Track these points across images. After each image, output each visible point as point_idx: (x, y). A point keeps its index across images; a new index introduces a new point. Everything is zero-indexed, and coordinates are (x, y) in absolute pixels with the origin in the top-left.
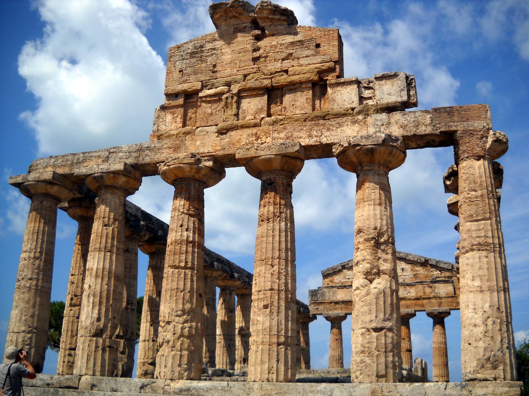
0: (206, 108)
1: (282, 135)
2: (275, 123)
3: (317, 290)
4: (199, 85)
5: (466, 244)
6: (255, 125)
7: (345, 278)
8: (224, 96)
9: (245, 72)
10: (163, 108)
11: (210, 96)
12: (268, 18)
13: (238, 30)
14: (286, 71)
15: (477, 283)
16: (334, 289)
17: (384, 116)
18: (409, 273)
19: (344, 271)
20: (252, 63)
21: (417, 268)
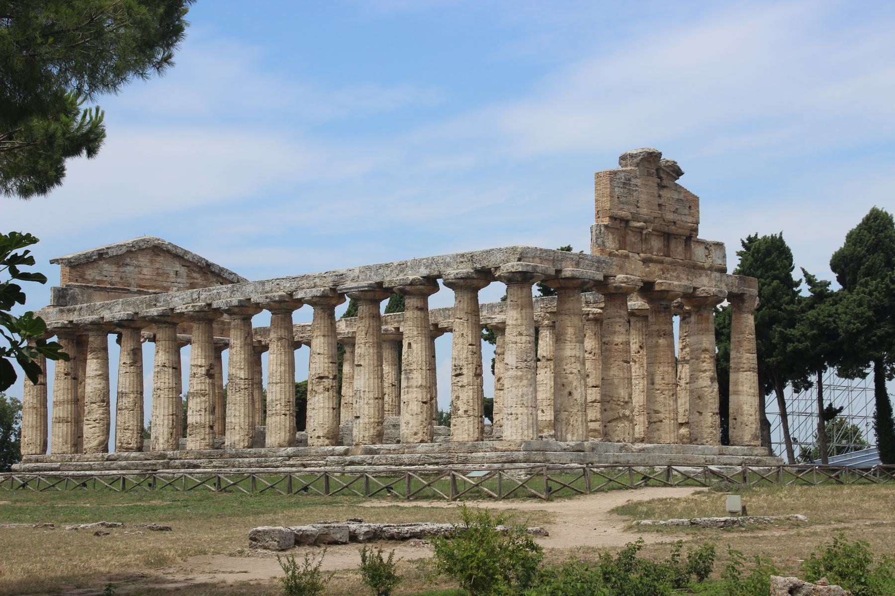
0: (632, 238)
1: (675, 274)
2: (671, 263)
3: (66, 289)
4: (630, 217)
5: (745, 366)
6: (662, 262)
7: (100, 274)
8: (644, 232)
9: (655, 215)
10: (606, 227)
11: (636, 227)
12: (668, 173)
13: (650, 174)
14: (675, 223)
15: (752, 391)
16: (90, 291)
17: (718, 274)
18: (184, 281)
19: (101, 262)
20: (657, 208)
21: (195, 275)
